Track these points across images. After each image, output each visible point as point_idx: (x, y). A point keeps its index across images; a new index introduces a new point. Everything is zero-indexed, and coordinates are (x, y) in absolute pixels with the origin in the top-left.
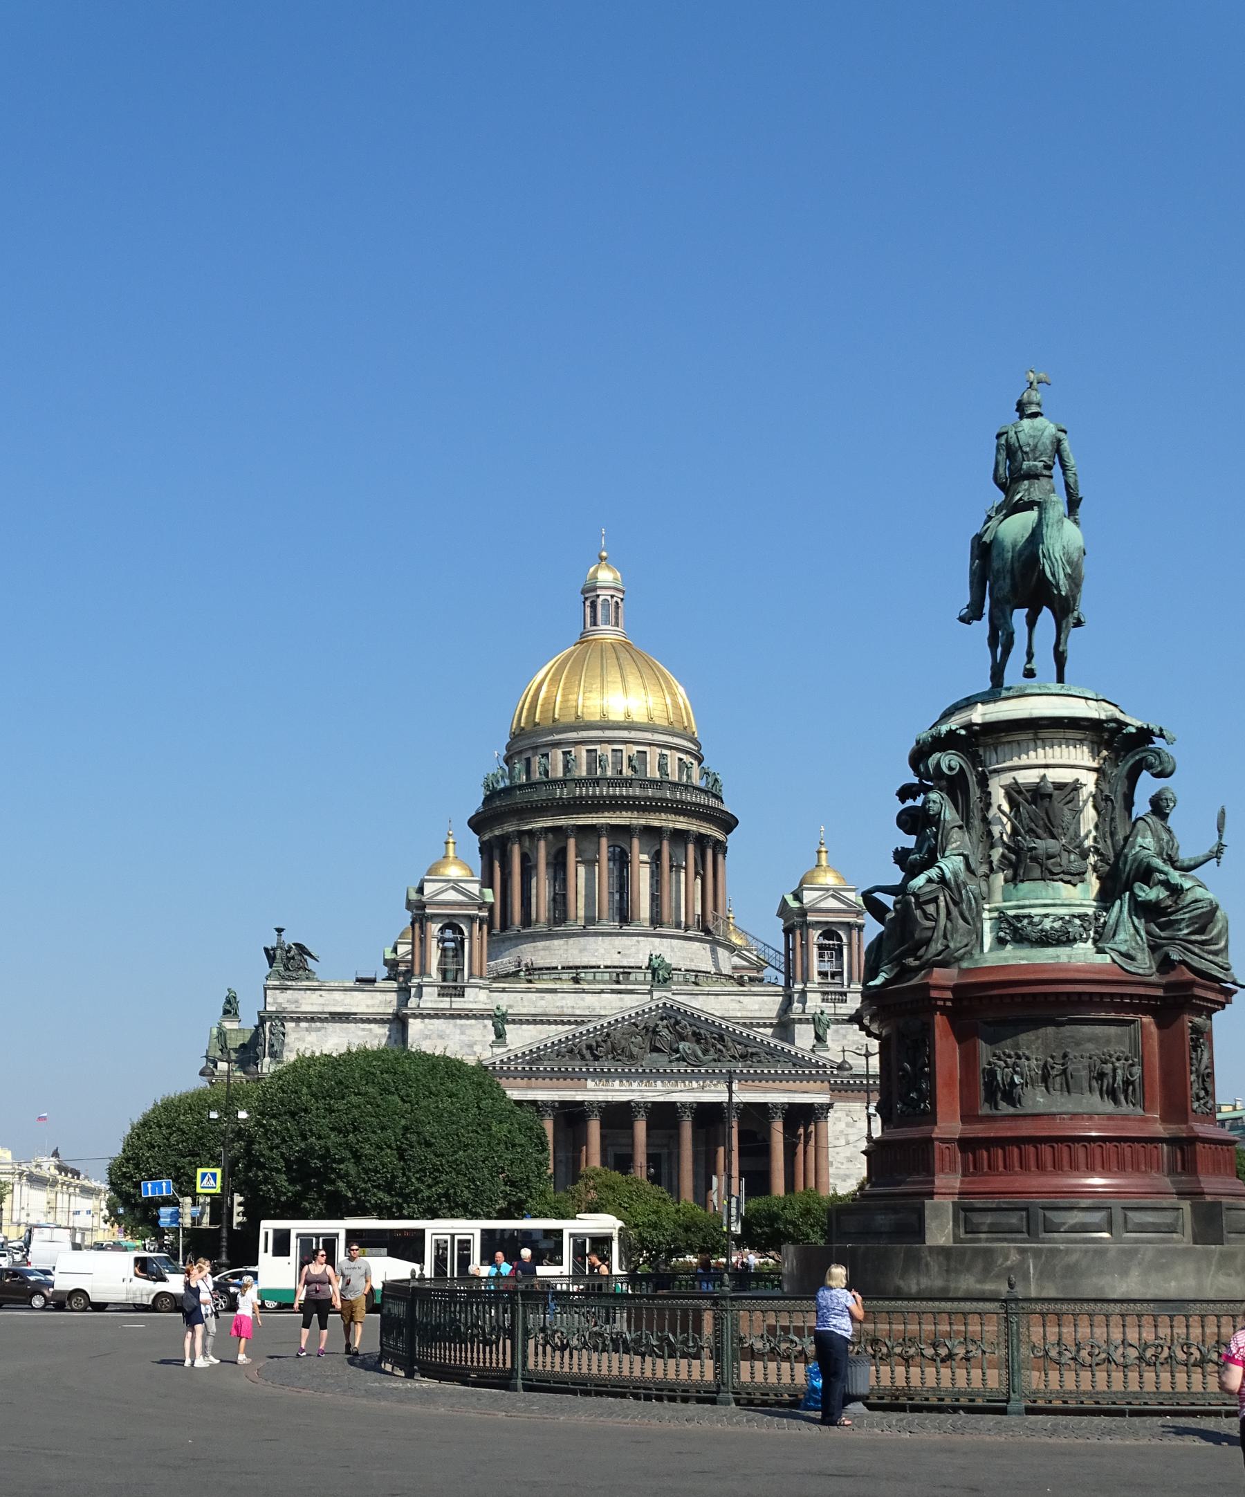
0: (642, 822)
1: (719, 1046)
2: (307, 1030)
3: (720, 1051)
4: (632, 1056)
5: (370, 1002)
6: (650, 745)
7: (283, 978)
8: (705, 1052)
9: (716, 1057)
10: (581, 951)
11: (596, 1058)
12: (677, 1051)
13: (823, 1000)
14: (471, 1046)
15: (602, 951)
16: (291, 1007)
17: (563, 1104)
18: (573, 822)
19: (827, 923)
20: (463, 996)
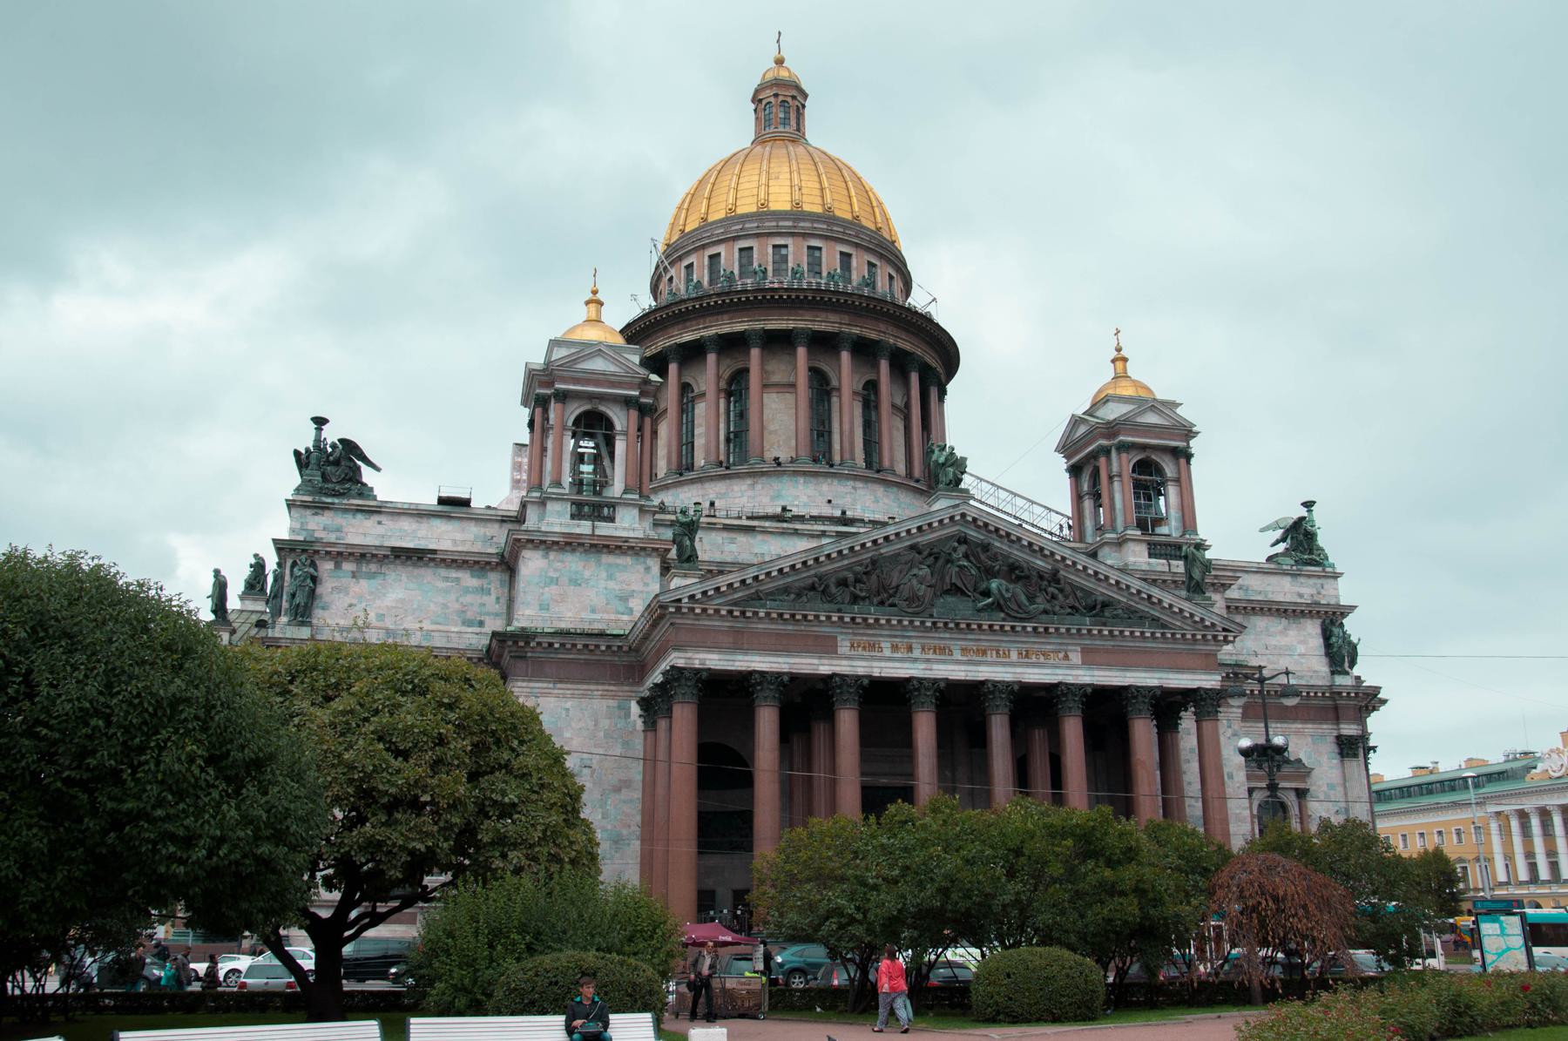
0: (856, 331)
1: (1050, 589)
2: (354, 575)
3: (1054, 597)
4: (913, 599)
5: (458, 536)
6: (857, 245)
7: (321, 491)
8: (1031, 599)
9: (1048, 606)
10: (773, 498)
11: (855, 599)
12: (987, 593)
13: (1150, 556)
14: (624, 599)
15: (804, 499)
16: (332, 538)
17: (795, 678)
18: (758, 326)
19: (1144, 447)
20: (612, 519)
